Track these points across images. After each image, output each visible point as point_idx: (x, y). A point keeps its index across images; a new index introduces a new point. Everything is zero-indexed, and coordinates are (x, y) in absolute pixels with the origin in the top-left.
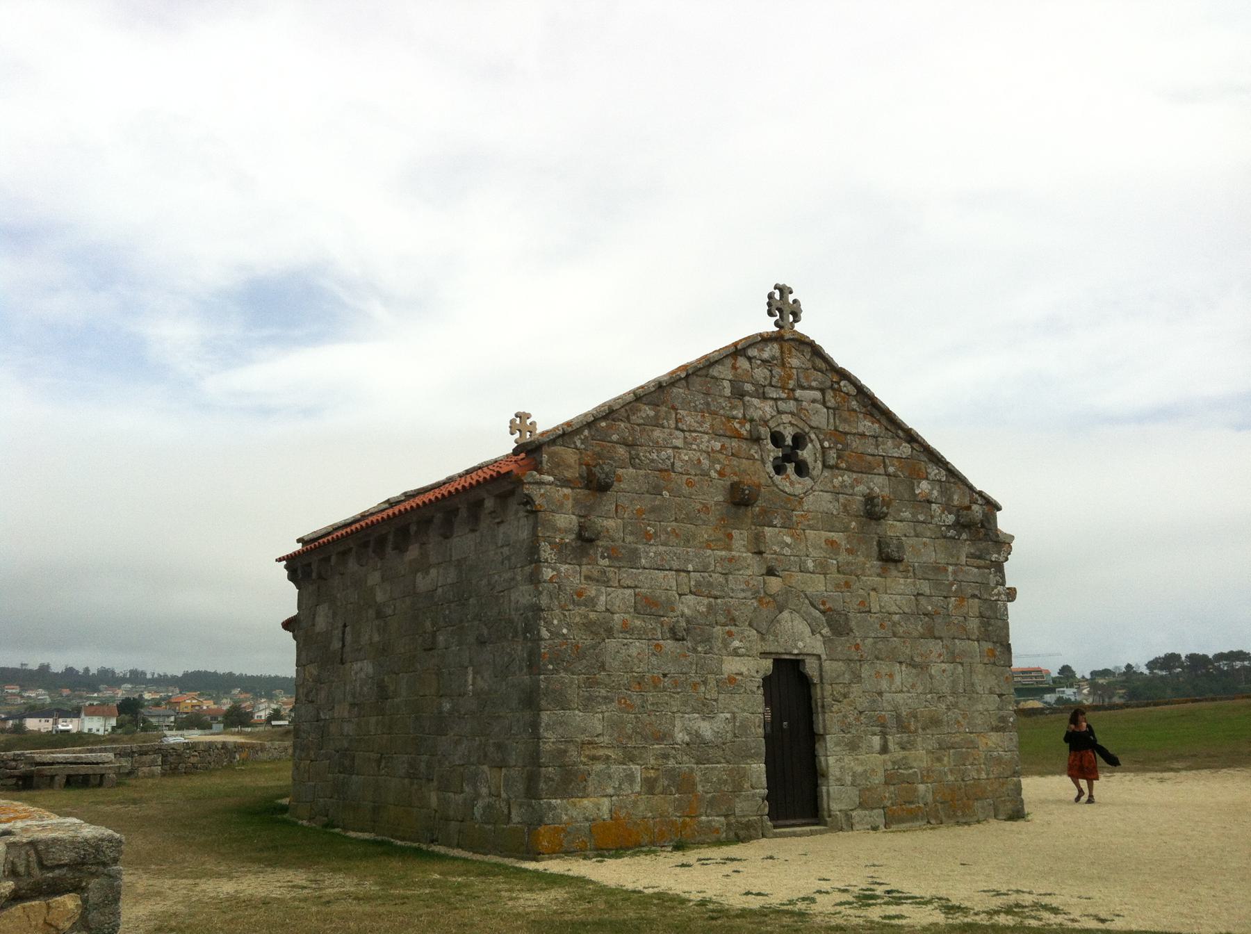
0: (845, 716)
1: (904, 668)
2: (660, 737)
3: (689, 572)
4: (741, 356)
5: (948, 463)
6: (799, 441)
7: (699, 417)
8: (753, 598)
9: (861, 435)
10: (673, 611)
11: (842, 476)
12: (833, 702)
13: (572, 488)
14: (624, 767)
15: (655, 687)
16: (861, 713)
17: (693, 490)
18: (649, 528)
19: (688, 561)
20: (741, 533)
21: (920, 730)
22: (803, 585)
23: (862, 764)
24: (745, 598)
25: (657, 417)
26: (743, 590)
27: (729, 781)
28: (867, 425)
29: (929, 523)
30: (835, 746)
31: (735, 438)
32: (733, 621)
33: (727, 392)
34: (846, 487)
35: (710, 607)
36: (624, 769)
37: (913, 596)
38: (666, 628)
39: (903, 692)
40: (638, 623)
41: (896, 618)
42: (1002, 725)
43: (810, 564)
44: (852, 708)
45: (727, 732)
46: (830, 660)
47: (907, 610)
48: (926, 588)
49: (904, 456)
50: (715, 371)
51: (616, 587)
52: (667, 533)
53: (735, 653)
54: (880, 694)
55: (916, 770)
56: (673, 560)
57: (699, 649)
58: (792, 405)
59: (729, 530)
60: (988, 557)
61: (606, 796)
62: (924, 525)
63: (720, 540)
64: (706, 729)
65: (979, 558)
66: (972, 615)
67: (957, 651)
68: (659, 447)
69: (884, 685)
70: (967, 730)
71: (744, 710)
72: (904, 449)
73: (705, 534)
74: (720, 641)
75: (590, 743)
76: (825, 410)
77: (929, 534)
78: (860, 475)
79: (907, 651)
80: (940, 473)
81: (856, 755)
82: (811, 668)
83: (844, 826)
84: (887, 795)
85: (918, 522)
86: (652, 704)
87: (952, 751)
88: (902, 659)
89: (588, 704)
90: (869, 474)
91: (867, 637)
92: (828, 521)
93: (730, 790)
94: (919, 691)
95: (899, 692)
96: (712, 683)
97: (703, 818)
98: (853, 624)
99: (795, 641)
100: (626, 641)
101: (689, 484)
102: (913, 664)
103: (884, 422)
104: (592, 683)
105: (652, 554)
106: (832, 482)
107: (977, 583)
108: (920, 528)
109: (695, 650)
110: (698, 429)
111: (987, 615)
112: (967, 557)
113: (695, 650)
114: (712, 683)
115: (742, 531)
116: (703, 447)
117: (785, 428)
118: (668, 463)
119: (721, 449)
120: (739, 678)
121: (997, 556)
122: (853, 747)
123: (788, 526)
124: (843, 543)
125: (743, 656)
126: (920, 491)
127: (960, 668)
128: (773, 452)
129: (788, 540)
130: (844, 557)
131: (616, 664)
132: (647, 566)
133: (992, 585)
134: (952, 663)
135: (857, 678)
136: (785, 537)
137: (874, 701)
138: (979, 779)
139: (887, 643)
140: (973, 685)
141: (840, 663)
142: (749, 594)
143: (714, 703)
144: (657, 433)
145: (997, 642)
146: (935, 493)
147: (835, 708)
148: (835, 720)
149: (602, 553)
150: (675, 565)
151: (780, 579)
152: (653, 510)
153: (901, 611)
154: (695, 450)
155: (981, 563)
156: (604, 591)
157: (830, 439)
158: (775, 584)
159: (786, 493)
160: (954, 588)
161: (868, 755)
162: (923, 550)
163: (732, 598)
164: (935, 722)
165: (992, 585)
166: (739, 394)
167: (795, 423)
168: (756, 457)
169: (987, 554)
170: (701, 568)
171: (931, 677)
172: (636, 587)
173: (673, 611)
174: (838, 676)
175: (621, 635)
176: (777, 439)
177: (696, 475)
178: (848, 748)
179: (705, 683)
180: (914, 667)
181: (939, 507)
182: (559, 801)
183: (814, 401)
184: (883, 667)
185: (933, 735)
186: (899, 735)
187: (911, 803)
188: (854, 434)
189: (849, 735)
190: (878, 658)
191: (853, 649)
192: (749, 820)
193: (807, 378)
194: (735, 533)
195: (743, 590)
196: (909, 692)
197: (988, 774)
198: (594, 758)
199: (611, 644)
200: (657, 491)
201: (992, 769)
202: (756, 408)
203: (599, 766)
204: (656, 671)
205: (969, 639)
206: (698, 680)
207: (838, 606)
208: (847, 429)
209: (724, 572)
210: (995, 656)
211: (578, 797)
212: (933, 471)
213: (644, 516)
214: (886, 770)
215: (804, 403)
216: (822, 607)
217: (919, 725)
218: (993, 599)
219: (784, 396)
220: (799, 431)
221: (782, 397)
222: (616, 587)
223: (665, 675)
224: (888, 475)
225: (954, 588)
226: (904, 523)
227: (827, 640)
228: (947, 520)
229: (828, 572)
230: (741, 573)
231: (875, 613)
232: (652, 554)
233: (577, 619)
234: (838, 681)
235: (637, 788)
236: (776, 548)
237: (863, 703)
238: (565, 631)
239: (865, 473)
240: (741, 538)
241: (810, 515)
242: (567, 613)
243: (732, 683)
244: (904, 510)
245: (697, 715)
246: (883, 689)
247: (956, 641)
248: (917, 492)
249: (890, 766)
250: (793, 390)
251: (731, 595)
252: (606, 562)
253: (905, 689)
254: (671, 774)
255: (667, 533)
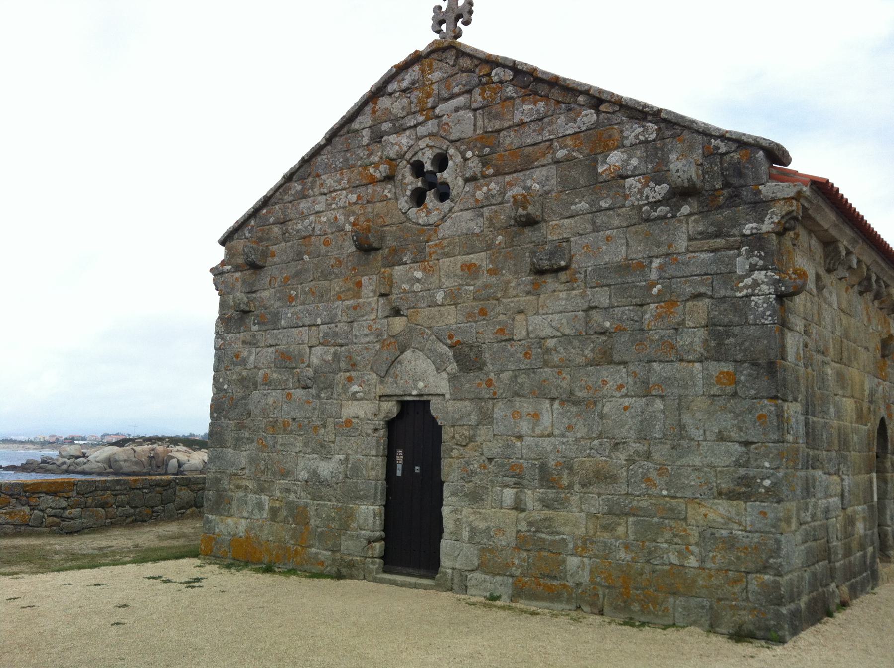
0: (468, 463)
1: (556, 404)
2: (284, 474)
3: (319, 325)
4: (383, 96)
5: (660, 111)
6: (441, 162)
7: (338, 176)
8: (377, 342)
9: (518, 125)
10: (303, 362)
11: (488, 185)
12: (455, 447)
13: (241, 271)
14: (257, 496)
15: (285, 430)
16: (490, 460)
17: (329, 248)
18: (292, 292)
19: (318, 315)
20: (370, 279)
21: (577, 487)
22: (430, 321)
23: (485, 519)
24: (369, 343)
25: (303, 189)
26: (366, 335)
27: (337, 519)
28: (527, 110)
29: (621, 207)
30: (450, 496)
31: (370, 184)
32: (354, 366)
33: (365, 140)
34: (493, 196)
35: (335, 354)
36: (256, 498)
37: (582, 311)
38: (296, 378)
39: (555, 436)
40: (275, 376)
41: (551, 343)
42: (743, 489)
43: (439, 296)
44: (477, 454)
45: (340, 472)
46: (454, 399)
47: (567, 331)
48: (602, 297)
49: (583, 129)
50: (355, 125)
51: (262, 347)
52: (306, 293)
53: (354, 397)
54: (520, 437)
55: (565, 537)
56: (306, 317)
57: (323, 395)
58: (431, 126)
59: (358, 278)
60: (735, 231)
61: (243, 518)
62: (611, 212)
63: (349, 290)
64: (326, 468)
65: (717, 235)
66: (691, 324)
67: (653, 379)
68: (303, 216)
69: (525, 427)
70: (664, 492)
71: (357, 453)
72: (585, 119)
73: (337, 286)
74: (341, 386)
75: (236, 475)
76: (471, 115)
77: (616, 222)
78: (514, 175)
79: (564, 384)
80: (646, 129)
81: (478, 508)
82: (436, 408)
83: (456, 587)
84: (516, 562)
85: (601, 210)
86: (281, 445)
87: (631, 519)
88: (555, 393)
89: (238, 443)
90: (527, 169)
91: (502, 371)
92: (470, 242)
93: (337, 527)
94: (579, 435)
95: (549, 436)
96: (331, 427)
97: (314, 550)
98: (487, 356)
99: (415, 381)
100: (265, 392)
101: (327, 243)
102: (570, 399)
103: (556, 94)
104: (241, 427)
105: (289, 315)
106: (474, 196)
107: (706, 274)
108: (600, 219)
109: (318, 397)
110: (337, 188)
111: (726, 320)
112: (690, 239)
113: (318, 397)
114: (331, 427)
115: (371, 277)
116: (341, 204)
117: (423, 154)
118: (310, 228)
119: (357, 200)
120: (356, 421)
121: (754, 225)
122: (475, 497)
123: (420, 259)
124: (484, 264)
125: (361, 399)
126: (606, 167)
127: (659, 404)
128: (412, 182)
129: (419, 275)
130: (484, 279)
131: (257, 411)
132: (285, 326)
133: (739, 272)
134: (644, 396)
135: (486, 418)
136: (415, 273)
137: (508, 446)
138: (683, 566)
139: (533, 375)
140: (683, 427)
141: (467, 403)
142: (372, 338)
143: (332, 445)
144: (304, 205)
145: (742, 362)
146: (634, 161)
147: (455, 453)
148: (455, 466)
149: (254, 320)
150: (307, 321)
151: (404, 318)
152: (297, 274)
153: (559, 334)
154: (334, 209)
155: (720, 242)
156: (254, 351)
157: (475, 146)
158: (398, 323)
159: (419, 224)
160: (655, 291)
161: (493, 510)
162: (604, 247)
163: (355, 344)
164: (603, 477)
165: (739, 272)
166: (378, 137)
167: (432, 144)
168: (389, 196)
169: (734, 226)
170: (328, 320)
171: (602, 416)
172: (277, 345)
173: (303, 362)
174: (462, 417)
175: (262, 387)
176: (417, 168)
177: (332, 233)
178: (466, 499)
179: (324, 426)
180: (577, 403)
181: (639, 181)
182: (214, 517)
183: (457, 110)
184: (526, 406)
185: (600, 495)
186: (541, 490)
187: (555, 578)
188: (510, 127)
189: (471, 484)
190: (517, 394)
191: (484, 385)
192: (352, 560)
193: (448, 88)
194: (364, 280)
195: (366, 335)
196: (563, 436)
197: (703, 561)
198: (238, 487)
199: (256, 394)
200: (299, 257)
201: (711, 554)
202: (393, 144)
203: (241, 494)
204: (286, 417)
205: (682, 360)
206: (319, 423)
207: (469, 339)
208: (497, 125)
209: (349, 320)
210: (736, 383)
211: (224, 516)
212: (633, 132)
213: (289, 282)
214: (518, 531)
215: (444, 118)
216: (449, 342)
217: (576, 479)
218: (738, 294)
219: (421, 119)
220: (438, 151)
221: (419, 121)
222: (262, 347)
223: (294, 420)
224: (557, 162)
225: (655, 291)
226: (577, 218)
227: (453, 378)
228: (651, 195)
229: (459, 301)
230: (365, 318)
231: (520, 341)
232: (289, 315)
233: (235, 377)
234: (460, 423)
235: (265, 516)
236: (405, 286)
237: (494, 448)
238: (226, 387)
239: (522, 171)
240: (369, 284)
241: (445, 242)
242: (228, 373)
243: (349, 426)
244: (577, 200)
245: (316, 456)
246: (523, 433)
247: (655, 365)
248: (600, 171)
249: (523, 526)
250: (433, 108)
251: (355, 341)
252: (256, 327)
253: (557, 432)
254: (291, 506)
255: (306, 293)
